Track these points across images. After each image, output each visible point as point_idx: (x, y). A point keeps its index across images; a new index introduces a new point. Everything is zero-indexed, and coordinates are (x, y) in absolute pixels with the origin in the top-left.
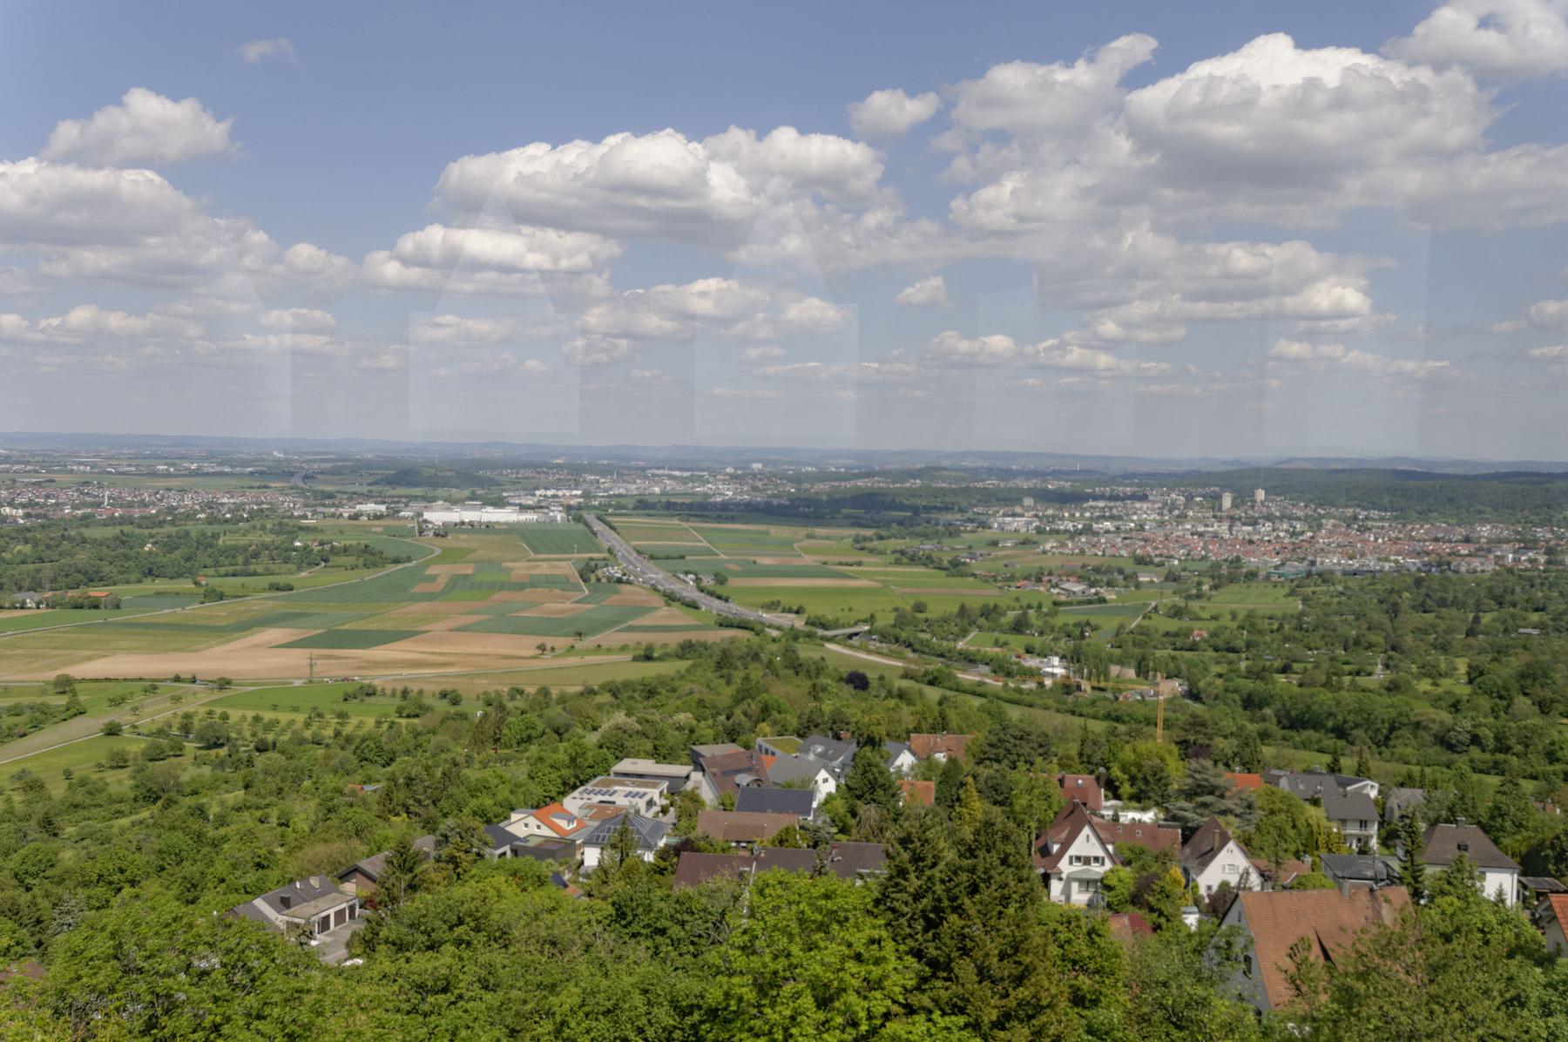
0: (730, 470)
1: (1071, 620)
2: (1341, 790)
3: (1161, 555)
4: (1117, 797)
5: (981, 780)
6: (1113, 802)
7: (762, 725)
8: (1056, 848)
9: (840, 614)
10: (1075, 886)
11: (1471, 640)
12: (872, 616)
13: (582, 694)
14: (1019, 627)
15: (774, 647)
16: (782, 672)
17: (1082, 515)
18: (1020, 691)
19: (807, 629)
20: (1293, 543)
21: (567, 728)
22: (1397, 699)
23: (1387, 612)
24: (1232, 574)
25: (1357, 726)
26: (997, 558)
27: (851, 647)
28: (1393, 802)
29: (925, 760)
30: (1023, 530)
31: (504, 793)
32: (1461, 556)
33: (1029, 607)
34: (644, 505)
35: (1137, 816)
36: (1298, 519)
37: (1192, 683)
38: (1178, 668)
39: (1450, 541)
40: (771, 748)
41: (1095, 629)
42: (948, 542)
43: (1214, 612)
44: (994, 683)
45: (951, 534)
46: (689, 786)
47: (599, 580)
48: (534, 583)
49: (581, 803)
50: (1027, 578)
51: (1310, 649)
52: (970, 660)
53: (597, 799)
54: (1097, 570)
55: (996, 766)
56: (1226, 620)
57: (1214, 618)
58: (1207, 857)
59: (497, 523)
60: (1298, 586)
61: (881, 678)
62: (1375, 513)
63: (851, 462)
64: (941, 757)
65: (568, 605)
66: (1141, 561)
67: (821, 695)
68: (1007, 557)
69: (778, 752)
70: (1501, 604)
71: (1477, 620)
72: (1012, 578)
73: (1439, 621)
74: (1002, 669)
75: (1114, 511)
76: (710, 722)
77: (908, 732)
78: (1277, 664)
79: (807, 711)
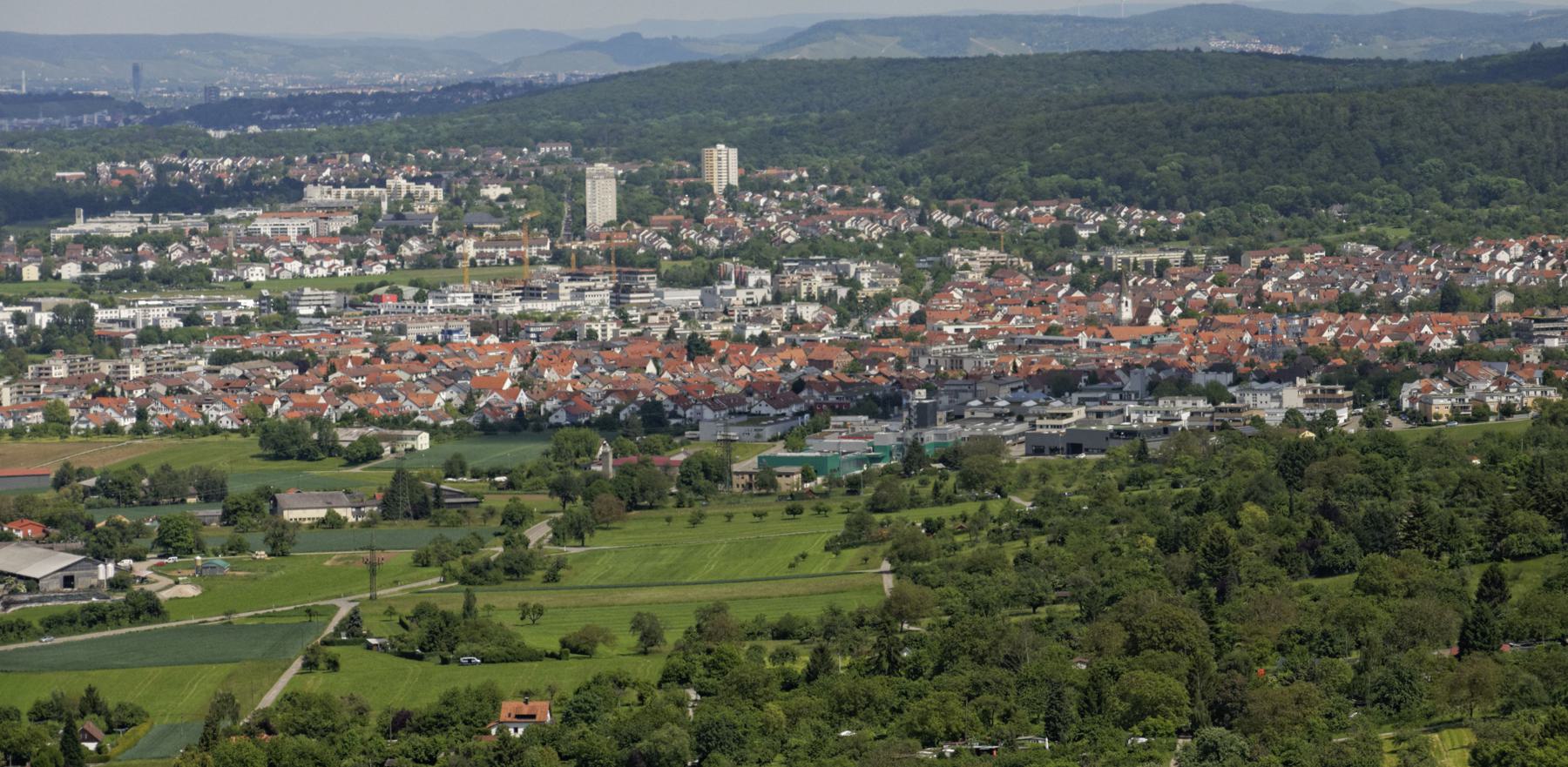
3: (362, 417)
11: (1479, 664)
17: (46, 274)
20: (851, 345)
23: (1193, 582)
32: (1428, 358)
36: (867, 251)
39: (1393, 307)
41: (119, 723)
43: (573, 625)
51: (929, 742)
54: (117, 490)
57: (576, 648)
60: (875, 506)
62: (1130, 218)
71: (1494, 587)
73: (1368, 603)
75: (176, 252)
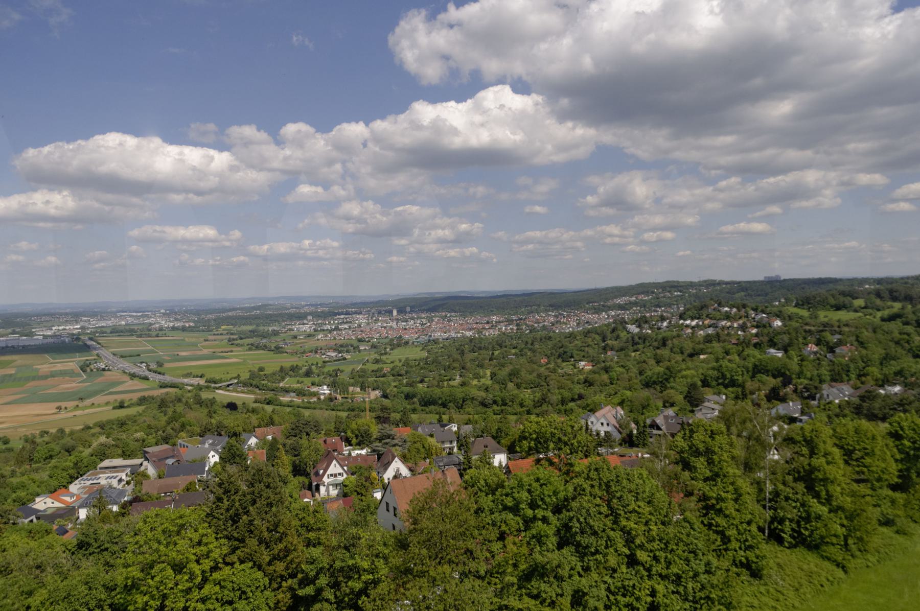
0: (163, 311)
1: (331, 369)
2: (442, 429)
4: (350, 445)
5: (287, 446)
6: (349, 447)
7: (182, 433)
8: (321, 472)
9: (222, 376)
10: (331, 487)
11: (491, 362)
12: (239, 375)
13: (83, 429)
14: (308, 374)
15: (189, 395)
16: (194, 406)
18: (309, 403)
19: (206, 384)
21: (73, 448)
22: (465, 389)
24: (400, 343)
25: (450, 402)
26: (297, 344)
27: (229, 391)
28: (462, 432)
29: (262, 440)
30: (308, 331)
31: (33, 488)
33: (312, 364)
34: (116, 331)
35: (359, 452)
36: (424, 318)
37: (384, 391)
38: (378, 385)
40: (186, 444)
41: (342, 372)
42: (273, 338)
44: (297, 400)
45: (275, 335)
46: (142, 468)
47: (92, 370)
48: (53, 375)
49: (79, 486)
50: (311, 352)
52: (286, 391)
53: (88, 483)
54: (342, 346)
55: (294, 438)
56: (397, 363)
58: (386, 466)
59: (29, 345)
61: (244, 404)
62: (453, 314)
63: (225, 304)
64: (270, 437)
65: (74, 385)
66: (360, 340)
67: (214, 415)
68: (300, 343)
69: (189, 445)
70: (501, 347)
71: (493, 354)
72: (304, 352)
74: (300, 393)
76: (154, 435)
77: (254, 427)
78: (418, 379)
79: (204, 423)
